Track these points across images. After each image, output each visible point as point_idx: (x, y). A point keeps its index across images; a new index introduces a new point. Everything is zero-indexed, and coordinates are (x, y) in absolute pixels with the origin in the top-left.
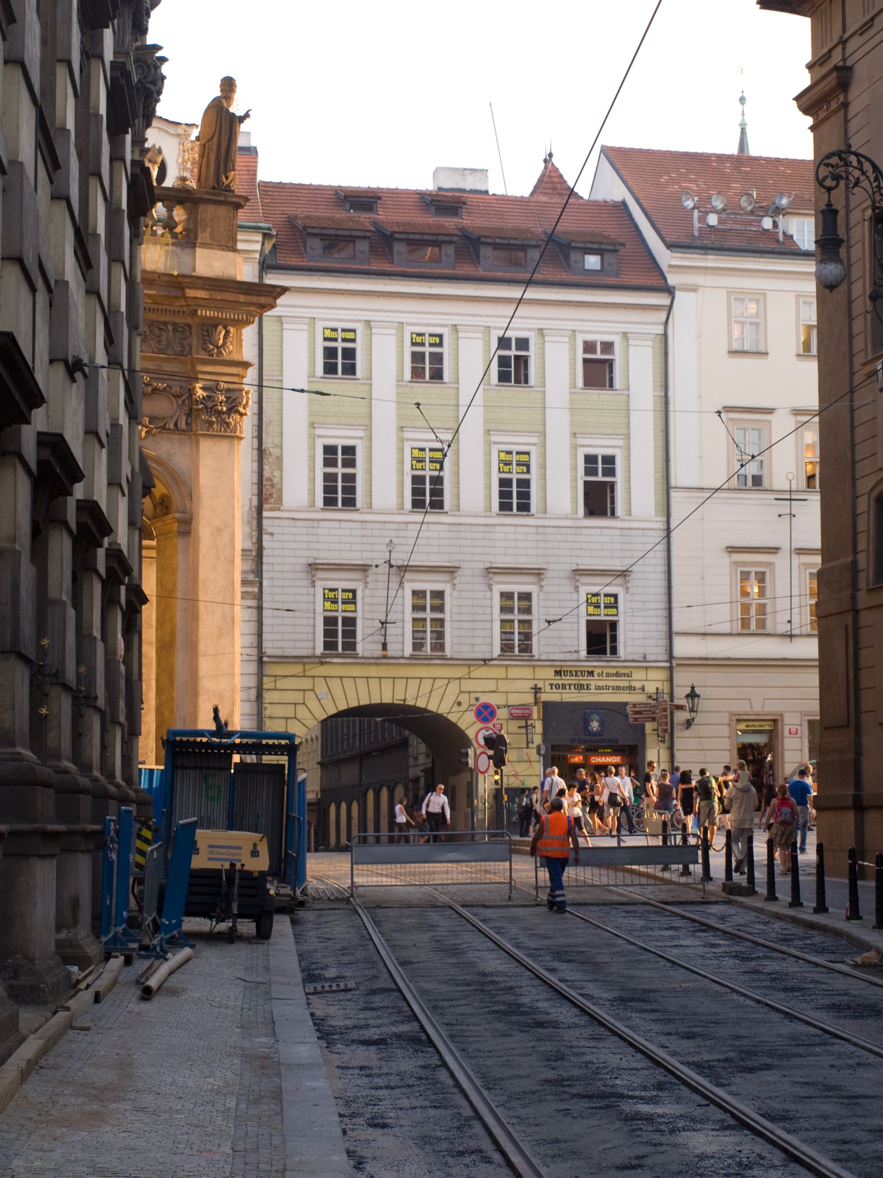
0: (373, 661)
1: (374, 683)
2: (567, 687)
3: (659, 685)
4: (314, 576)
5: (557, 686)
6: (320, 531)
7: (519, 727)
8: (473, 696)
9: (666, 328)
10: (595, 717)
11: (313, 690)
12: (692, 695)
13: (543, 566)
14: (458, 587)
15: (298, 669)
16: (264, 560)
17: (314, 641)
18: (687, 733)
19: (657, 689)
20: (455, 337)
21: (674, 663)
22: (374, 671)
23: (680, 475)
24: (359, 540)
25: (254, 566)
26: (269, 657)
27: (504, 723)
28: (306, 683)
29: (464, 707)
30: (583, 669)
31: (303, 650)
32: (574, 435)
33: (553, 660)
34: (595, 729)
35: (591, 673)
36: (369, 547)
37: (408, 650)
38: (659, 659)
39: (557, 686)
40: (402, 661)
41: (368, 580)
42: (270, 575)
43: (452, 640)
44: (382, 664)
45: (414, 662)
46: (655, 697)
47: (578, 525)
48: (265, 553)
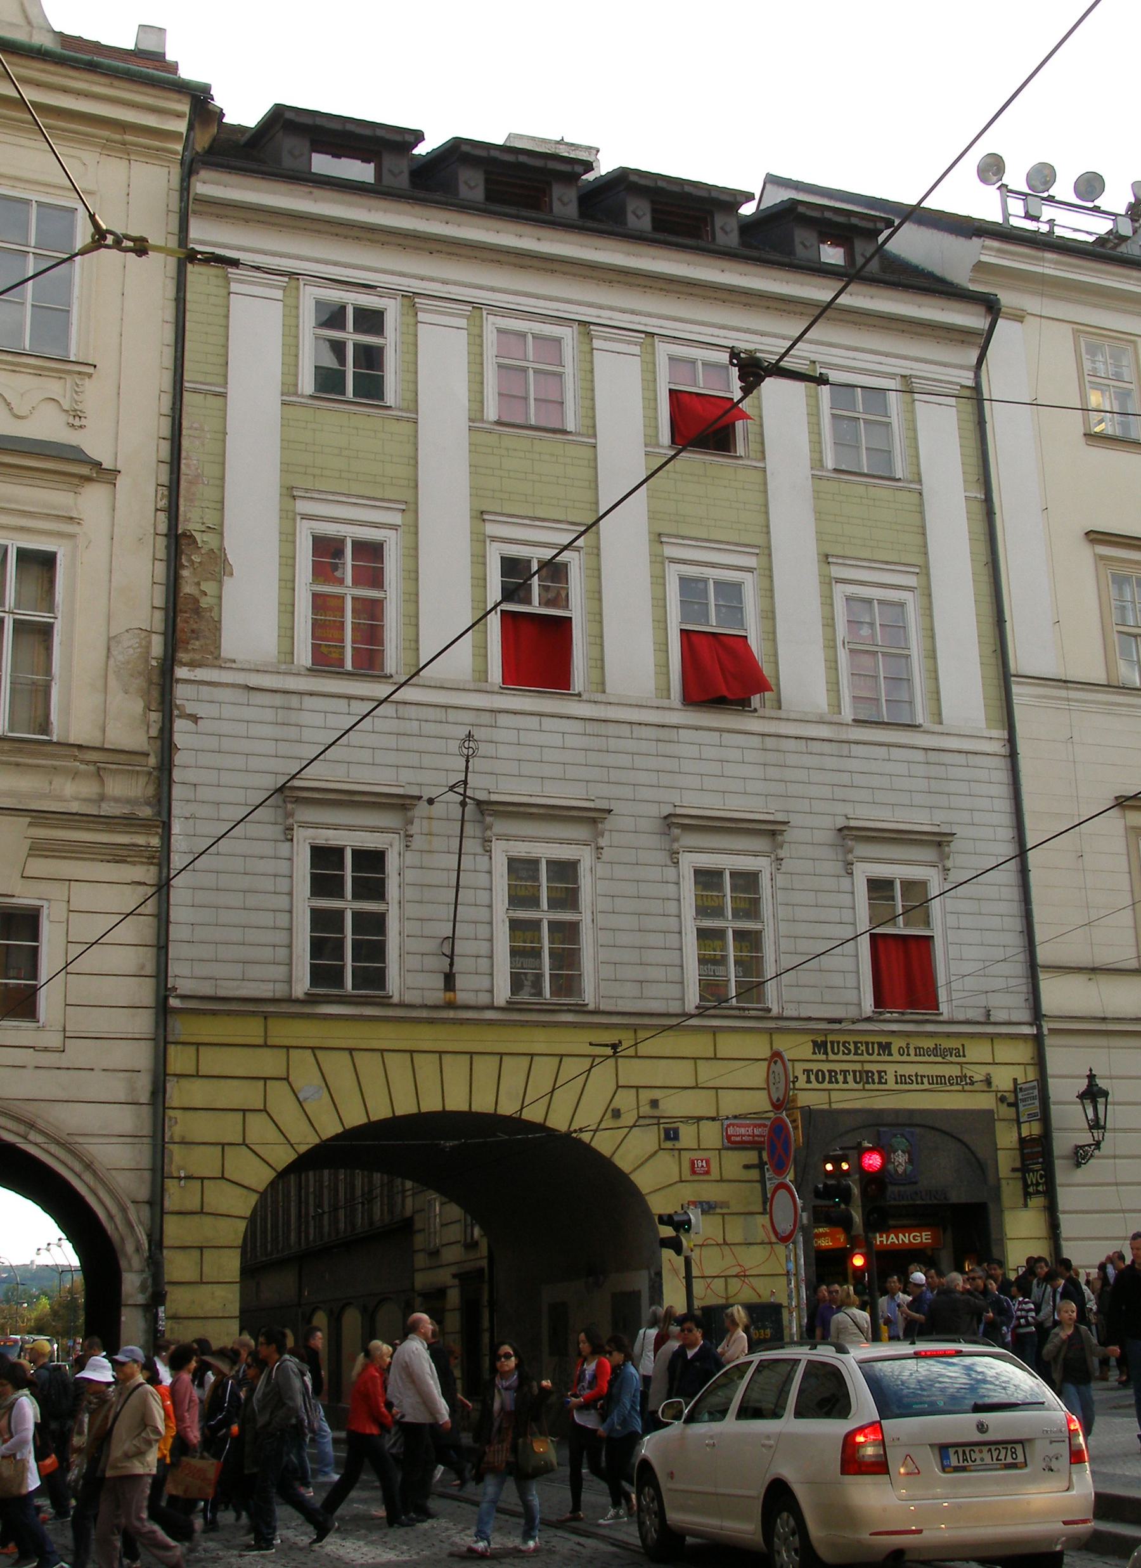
0: (424, 1014)
1: (427, 1066)
2: (840, 1078)
3: (1018, 1073)
4: (290, 815)
5: (820, 1076)
6: (306, 718)
7: (747, 1167)
8: (646, 1096)
9: (977, 377)
10: (899, 1142)
11: (287, 1079)
12: (1093, 1093)
13: (780, 817)
14: (607, 854)
15: (252, 1030)
16: (177, 775)
17: (290, 964)
18: (1080, 1175)
19: (1015, 1080)
20: (587, 348)
21: (1046, 1026)
22: (426, 1038)
23: (1027, 655)
24: (391, 741)
25: (151, 791)
26: (183, 997)
27: (713, 1156)
28: (269, 1063)
29: (628, 1119)
30: (870, 1039)
31: (261, 984)
32: (825, 559)
33: (810, 1019)
34: (900, 1170)
35: (886, 1048)
36: (413, 759)
37: (503, 993)
38: (1014, 1019)
39: (820, 1076)
40: (489, 1015)
41: (414, 829)
42: (188, 810)
43: (597, 971)
44: (444, 1021)
45: (516, 1016)
46: (1011, 1099)
47: (844, 737)
48: (178, 759)
